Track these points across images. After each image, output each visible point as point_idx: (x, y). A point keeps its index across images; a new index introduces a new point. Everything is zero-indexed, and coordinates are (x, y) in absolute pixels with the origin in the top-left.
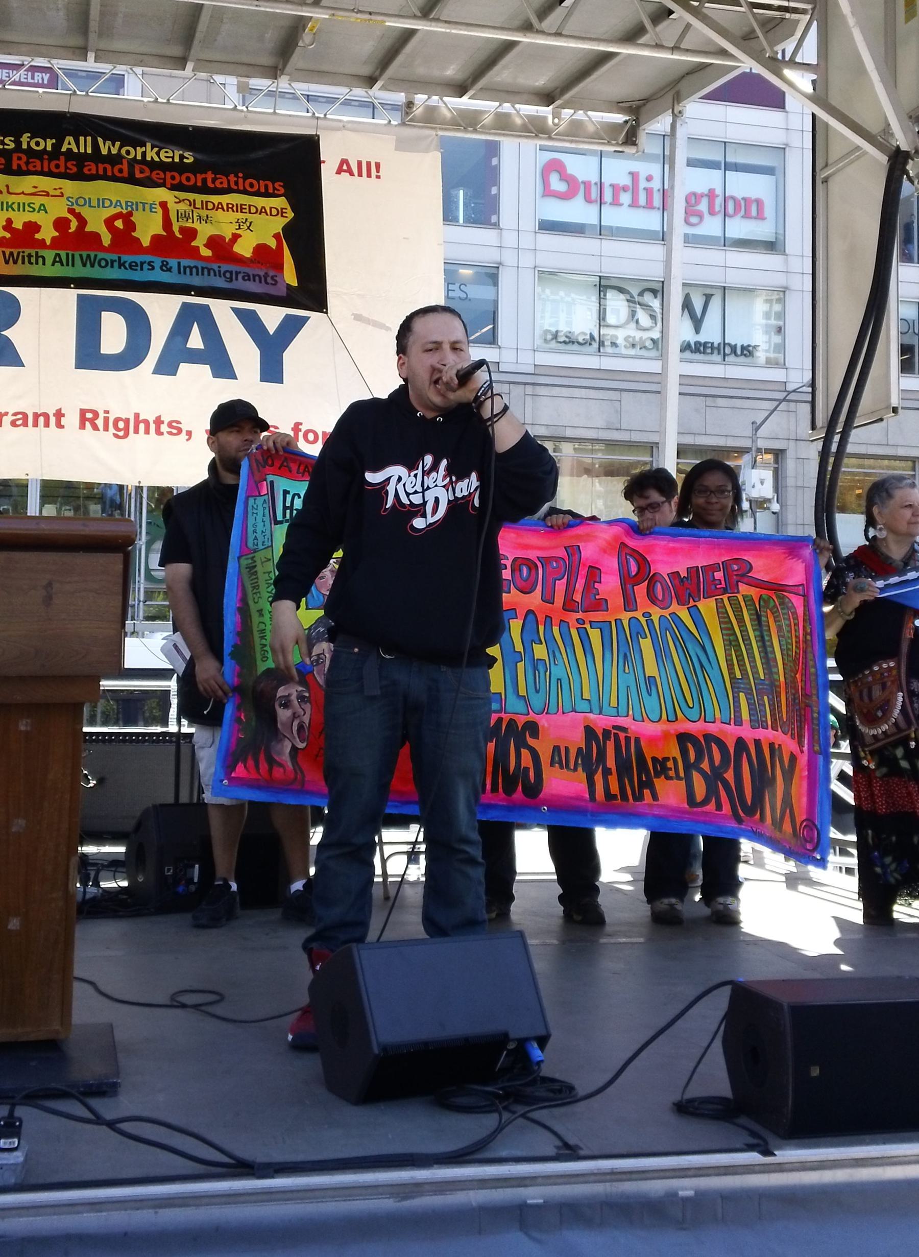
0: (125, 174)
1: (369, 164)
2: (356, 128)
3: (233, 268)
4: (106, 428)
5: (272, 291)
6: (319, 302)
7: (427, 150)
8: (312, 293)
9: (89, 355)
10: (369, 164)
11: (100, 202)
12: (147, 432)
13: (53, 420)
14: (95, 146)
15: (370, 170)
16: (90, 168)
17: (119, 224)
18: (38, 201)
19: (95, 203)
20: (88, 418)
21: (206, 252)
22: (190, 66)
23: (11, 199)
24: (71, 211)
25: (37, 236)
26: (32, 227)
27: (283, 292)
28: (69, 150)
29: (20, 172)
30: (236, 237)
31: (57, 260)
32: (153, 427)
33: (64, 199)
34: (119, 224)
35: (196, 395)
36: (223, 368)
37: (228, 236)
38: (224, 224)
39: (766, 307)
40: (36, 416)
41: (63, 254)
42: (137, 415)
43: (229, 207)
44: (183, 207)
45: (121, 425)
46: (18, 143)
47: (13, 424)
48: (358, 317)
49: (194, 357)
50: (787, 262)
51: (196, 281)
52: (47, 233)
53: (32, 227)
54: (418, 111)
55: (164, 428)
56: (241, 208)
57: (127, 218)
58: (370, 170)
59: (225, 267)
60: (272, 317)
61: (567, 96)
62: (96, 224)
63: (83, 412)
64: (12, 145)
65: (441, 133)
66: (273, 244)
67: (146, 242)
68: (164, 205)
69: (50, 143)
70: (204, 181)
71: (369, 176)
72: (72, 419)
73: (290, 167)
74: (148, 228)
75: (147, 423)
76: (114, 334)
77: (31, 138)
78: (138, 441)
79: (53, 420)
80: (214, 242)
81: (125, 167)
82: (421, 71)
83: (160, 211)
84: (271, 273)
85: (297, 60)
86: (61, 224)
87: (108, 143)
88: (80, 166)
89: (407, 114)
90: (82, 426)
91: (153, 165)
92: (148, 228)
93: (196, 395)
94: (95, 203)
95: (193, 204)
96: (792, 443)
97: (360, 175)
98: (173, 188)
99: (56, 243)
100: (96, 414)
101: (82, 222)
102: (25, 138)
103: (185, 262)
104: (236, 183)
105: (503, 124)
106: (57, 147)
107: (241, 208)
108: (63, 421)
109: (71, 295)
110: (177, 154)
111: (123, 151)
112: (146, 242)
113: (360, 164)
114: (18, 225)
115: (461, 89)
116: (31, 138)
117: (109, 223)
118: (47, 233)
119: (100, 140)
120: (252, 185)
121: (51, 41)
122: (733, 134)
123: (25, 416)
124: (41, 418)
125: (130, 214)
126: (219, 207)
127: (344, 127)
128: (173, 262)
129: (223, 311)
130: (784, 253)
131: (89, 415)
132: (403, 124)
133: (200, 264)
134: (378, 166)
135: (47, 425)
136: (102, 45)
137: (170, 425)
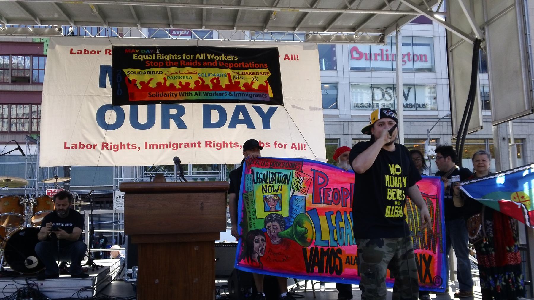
0: (216, 65)
1: (295, 56)
2: (290, 44)
3: (252, 93)
4: (214, 147)
5: (265, 99)
6: (280, 101)
7: (314, 49)
8: (278, 100)
9: (207, 124)
10: (295, 56)
11: (209, 74)
12: (227, 147)
13: (197, 145)
14: (206, 57)
15: (295, 58)
16: (205, 64)
17: (215, 81)
18: (189, 75)
19: (207, 75)
20: (208, 144)
21: (243, 89)
22: (235, 28)
23: (181, 75)
24: (200, 78)
25: (190, 87)
26: (188, 84)
27: (269, 100)
28: (198, 58)
29: (183, 66)
30: (252, 83)
31: (196, 94)
32: (229, 145)
33: (197, 75)
34: (215, 81)
35: (242, 134)
36: (251, 125)
37: (250, 83)
38: (249, 79)
39: (429, 90)
40: (192, 144)
41: (198, 92)
42: (224, 142)
43: (250, 73)
44: (235, 74)
45: (219, 145)
46: (182, 57)
47: (185, 147)
48: (293, 106)
49: (241, 122)
50: (436, 75)
51: (240, 98)
52: (192, 86)
53: (188, 84)
54: (310, 37)
55: (233, 145)
56: (254, 73)
57: (217, 79)
58: (295, 58)
59: (249, 93)
60: (265, 108)
61: (360, 28)
62: (208, 82)
63: (206, 142)
64: (180, 58)
65: (318, 44)
66: (264, 84)
67: (224, 87)
68: (229, 74)
69: (192, 56)
70: (241, 65)
71: (295, 59)
72: (203, 145)
73: (269, 59)
74: (224, 82)
75: (227, 144)
76: (215, 116)
77: (186, 55)
78: (225, 150)
79: (197, 145)
80: (245, 85)
81: (216, 63)
82: (310, 24)
83: (228, 76)
84: (265, 94)
85: (270, 24)
86: (197, 82)
87: (210, 55)
88: (202, 64)
89: (307, 38)
90: (206, 147)
91: (225, 62)
92: (224, 82)
93: (242, 134)
94: (207, 75)
95: (238, 73)
96: (442, 136)
97: (292, 59)
98: (231, 69)
99: (195, 89)
100: (211, 142)
101: (203, 82)
102: (184, 55)
103: (236, 92)
104: (252, 65)
105: (339, 39)
106: (194, 57)
107: (254, 73)
108: (200, 145)
109: (201, 105)
110: (232, 57)
111: (215, 58)
112: (224, 87)
113: (292, 56)
114: (183, 84)
115: (324, 29)
116: (186, 55)
117: (212, 81)
118: (192, 86)
119: (208, 55)
120: (257, 66)
121: (190, 23)
122: (415, 34)
123: (188, 144)
124: (193, 145)
125: (218, 78)
126: (245, 74)
127: (286, 44)
128: (233, 93)
129: (249, 107)
130: (435, 72)
131: (208, 143)
132: (305, 41)
133: (241, 92)
134: (298, 56)
135: (195, 147)
136: (207, 23)
137: (234, 144)
